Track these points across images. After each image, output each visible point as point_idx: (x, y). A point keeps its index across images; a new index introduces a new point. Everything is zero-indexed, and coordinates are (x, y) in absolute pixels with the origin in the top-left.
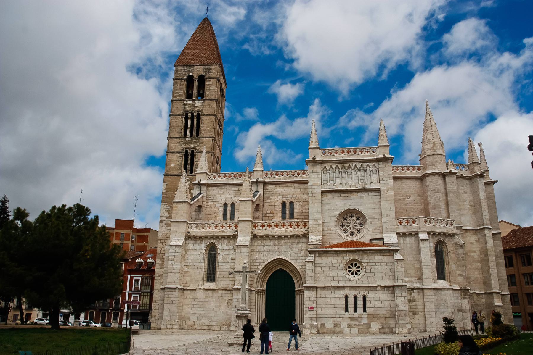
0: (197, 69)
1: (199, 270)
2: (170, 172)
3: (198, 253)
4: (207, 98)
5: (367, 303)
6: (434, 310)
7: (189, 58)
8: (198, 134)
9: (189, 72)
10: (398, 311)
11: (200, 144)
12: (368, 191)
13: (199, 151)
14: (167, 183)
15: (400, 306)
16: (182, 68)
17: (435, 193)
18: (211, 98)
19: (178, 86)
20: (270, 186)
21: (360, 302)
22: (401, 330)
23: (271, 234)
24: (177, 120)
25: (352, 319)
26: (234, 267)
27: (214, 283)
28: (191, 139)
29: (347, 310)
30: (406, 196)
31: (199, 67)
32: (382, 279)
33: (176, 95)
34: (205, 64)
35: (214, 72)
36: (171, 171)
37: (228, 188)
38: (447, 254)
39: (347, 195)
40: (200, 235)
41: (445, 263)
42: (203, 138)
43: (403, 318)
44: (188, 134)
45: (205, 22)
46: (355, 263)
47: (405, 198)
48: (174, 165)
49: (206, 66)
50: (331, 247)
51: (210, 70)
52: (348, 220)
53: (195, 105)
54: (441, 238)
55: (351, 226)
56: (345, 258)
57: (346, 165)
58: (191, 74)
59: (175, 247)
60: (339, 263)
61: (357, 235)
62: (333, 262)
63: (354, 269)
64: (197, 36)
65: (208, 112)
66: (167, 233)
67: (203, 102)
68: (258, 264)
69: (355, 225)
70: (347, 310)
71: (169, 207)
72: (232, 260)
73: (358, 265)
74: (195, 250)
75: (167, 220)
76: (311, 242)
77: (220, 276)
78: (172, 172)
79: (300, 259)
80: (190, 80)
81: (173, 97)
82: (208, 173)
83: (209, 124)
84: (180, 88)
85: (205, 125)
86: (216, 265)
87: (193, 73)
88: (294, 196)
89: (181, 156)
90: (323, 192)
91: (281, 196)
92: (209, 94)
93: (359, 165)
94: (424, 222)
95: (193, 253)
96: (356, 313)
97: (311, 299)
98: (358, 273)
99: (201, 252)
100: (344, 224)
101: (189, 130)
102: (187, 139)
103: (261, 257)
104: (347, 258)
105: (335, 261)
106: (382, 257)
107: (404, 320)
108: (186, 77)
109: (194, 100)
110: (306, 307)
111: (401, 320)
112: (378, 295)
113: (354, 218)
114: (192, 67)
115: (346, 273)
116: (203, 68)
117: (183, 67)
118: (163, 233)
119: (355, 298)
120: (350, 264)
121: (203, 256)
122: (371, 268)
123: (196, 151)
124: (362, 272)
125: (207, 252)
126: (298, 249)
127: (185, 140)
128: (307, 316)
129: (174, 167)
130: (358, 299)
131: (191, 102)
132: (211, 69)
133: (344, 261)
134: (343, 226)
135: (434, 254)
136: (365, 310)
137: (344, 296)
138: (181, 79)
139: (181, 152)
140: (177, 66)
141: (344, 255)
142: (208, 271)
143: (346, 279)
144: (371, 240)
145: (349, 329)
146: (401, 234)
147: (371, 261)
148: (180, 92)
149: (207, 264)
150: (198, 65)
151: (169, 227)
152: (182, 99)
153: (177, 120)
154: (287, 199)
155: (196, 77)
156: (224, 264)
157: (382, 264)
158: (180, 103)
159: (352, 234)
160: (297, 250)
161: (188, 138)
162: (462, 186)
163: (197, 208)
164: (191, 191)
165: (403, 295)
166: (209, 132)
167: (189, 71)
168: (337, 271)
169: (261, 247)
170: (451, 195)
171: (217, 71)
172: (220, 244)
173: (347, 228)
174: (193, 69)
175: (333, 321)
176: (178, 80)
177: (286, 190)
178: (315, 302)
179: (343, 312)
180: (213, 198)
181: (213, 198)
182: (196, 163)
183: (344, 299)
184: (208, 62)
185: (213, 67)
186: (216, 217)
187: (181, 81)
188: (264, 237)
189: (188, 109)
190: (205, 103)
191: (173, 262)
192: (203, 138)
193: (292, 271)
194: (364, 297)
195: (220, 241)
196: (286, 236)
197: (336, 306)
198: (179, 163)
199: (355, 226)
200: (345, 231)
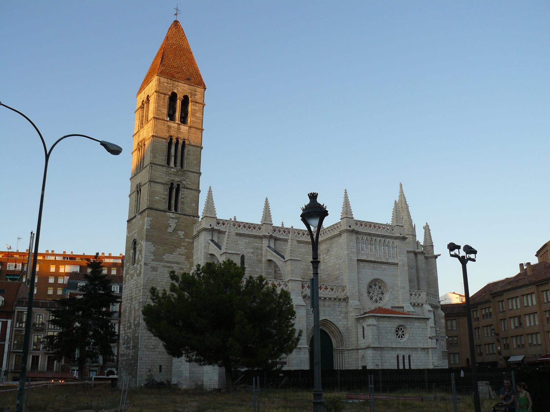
0: (182, 88)
2: (154, 206)
5: (411, 361)
7: (172, 69)
8: (182, 166)
11: (186, 178)
13: (186, 187)
14: (151, 219)
16: (166, 81)
18: (197, 126)
31: (183, 84)
34: (191, 84)
35: (200, 96)
36: (156, 205)
44: (172, 164)
46: (401, 327)
48: (158, 198)
49: (192, 87)
51: (196, 93)
52: (376, 287)
53: (180, 131)
56: (396, 323)
57: (374, 238)
58: (176, 91)
60: (392, 327)
63: (400, 333)
64: (173, 42)
66: (153, 279)
67: (189, 129)
71: (154, 248)
73: (403, 330)
75: (153, 262)
78: (156, 206)
79: (341, 321)
80: (173, 97)
85: (192, 158)
87: (177, 92)
89: (166, 189)
90: (358, 260)
93: (382, 239)
97: (377, 358)
98: (403, 337)
101: (173, 159)
102: (172, 169)
103: (309, 317)
104: (397, 323)
105: (389, 326)
113: (377, 287)
114: (177, 82)
118: (148, 278)
119: (403, 356)
120: (398, 329)
122: (413, 333)
123: (183, 186)
124: (407, 336)
126: (339, 312)
133: (394, 327)
134: (369, 293)
137: (397, 355)
138: (165, 94)
139: (167, 184)
141: (395, 320)
144: (392, 307)
146: (413, 304)
147: (413, 327)
148: (163, 110)
150: (182, 82)
151: (155, 271)
155: (180, 96)
159: (376, 301)
160: (338, 312)
164: (178, 233)
166: (195, 166)
170: (421, 272)
174: (177, 86)
178: (380, 361)
182: (182, 200)
184: (194, 83)
187: (164, 97)
189: (173, 133)
190: (191, 131)
193: (332, 332)
196: (330, 299)
197: (392, 364)
198: (165, 197)
200: (371, 298)
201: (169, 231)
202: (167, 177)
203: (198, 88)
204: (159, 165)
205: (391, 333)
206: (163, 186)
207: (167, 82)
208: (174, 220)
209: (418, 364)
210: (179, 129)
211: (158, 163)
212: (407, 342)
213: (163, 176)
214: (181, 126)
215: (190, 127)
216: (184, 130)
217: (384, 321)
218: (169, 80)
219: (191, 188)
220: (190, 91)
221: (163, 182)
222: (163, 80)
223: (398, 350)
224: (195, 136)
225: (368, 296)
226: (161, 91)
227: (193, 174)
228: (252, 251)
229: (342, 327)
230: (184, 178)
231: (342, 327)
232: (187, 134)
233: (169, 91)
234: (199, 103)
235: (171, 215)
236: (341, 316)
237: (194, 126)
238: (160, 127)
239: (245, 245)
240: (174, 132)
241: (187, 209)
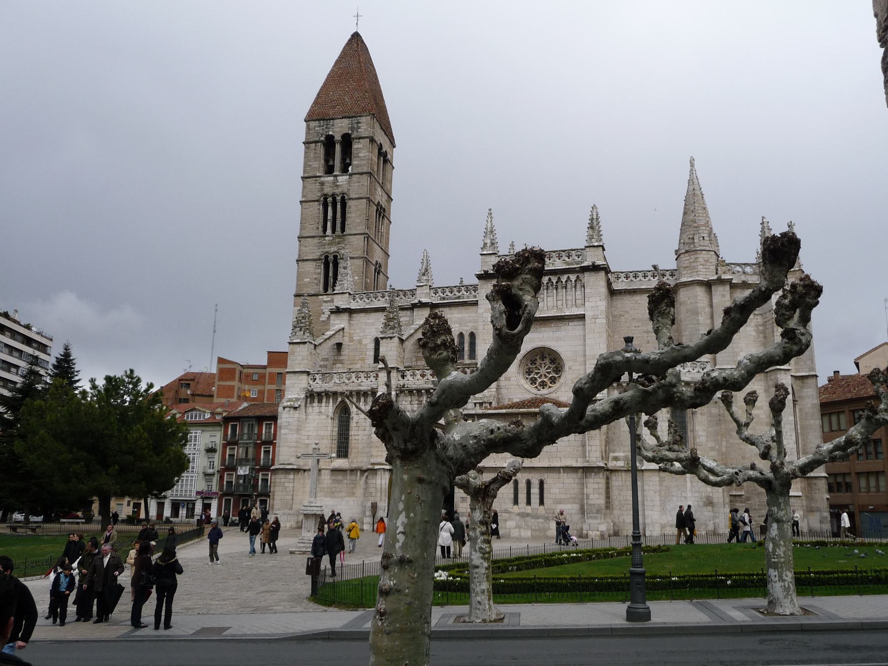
0: (340, 125)
1: (325, 441)
2: (302, 290)
3: (324, 417)
6: (658, 503)
8: (343, 229)
12: (567, 319)
15: (591, 497)
21: (535, 491)
24: (311, 209)
25: (523, 515)
27: (346, 460)
28: (333, 239)
29: (516, 502)
33: (308, 168)
35: (365, 127)
36: (305, 289)
38: (691, 415)
41: (689, 428)
42: (350, 235)
44: (329, 231)
48: (308, 280)
50: (511, 407)
51: (360, 125)
53: (338, 184)
58: (331, 133)
61: (550, 387)
65: (357, 194)
69: (548, 371)
70: (516, 502)
80: (329, 143)
81: (304, 172)
82: (352, 293)
83: (359, 212)
85: (354, 215)
86: (349, 433)
87: (333, 132)
89: (319, 266)
91: (458, 325)
96: (529, 508)
99: (328, 416)
101: (329, 224)
102: (327, 238)
107: (596, 518)
108: (323, 139)
109: (336, 176)
114: (331, 121)
117: (317, 122)
119: (529, 483)
121: (330, 421)
127: (325, 240)
129: (309, 282)
131: (332, 178)
132: (360, 123)
134: (529, 372)
136: (542, 502)
138: (316, 142)
140: (309, 121)
145: (517, 530)
149: (337, 433)
152: (318, 174)
153: (311, 209)
154: (466, 328)
155: (338, 137)
156: (360, 433)
159: (543, 385)
161: (328, 236)
163: (335, 347)
167: (326, 128)
171: (369, 126)
173: (535, 376)
174: (333, 125)
177: (464, 315)
185: (363, 120)
186: (363, 360)
187: (316, 146)
188: (414, 392)
189: (328, 190)
191: (287, 431)
192: (350, 235)
194: (542, 483)
198: (316, 276)
199: (548, 373)
200: (533, 381)
201: (321, 319)
202: (320, 250)
203: (362, 118)
206: (314, 263)
208: (329, 304)
210: (335, 184)
211: (308, 235)
213: (314, 250)
214: (338, 177)
215: (351, 175)
218: (322, 122)
219: (355, 256)
221: (316, 258)
224: (357, 184)
225: (527, 378)
226: (311, 140)
227: (356, 236)
230: (343, 245)
232: (347, 186)
233: (322, 136)
235: (325, 298)
237: (355, 171)
238: (310, 188)
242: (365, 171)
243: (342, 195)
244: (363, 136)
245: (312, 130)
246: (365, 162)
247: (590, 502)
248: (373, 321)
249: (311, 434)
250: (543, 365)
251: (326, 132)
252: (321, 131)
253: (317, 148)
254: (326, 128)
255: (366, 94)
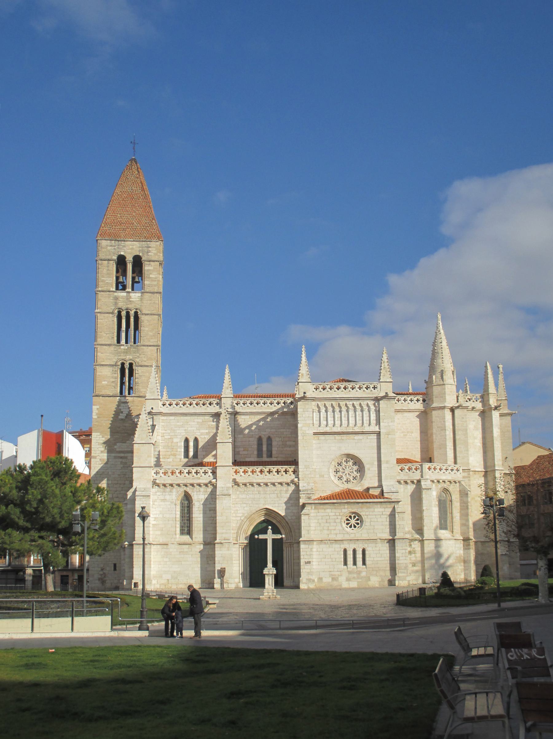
0: (131, 247)
4: (147, 291)
5: (367, 556)
7: (117, 227)
9: (119, 250)
10: (398, 564)
13: (140, 364)
15: (401, 558)
17: (442, 430)
19: (105, 270)
20: (243, 417)
22: (401, 582)
23: (255, 481)
26: (212, 518)
29: (345, 563)
30: (408, 432)
31: (133, 242)
32: (383, 533)
33: (102, 283)
34: (141, 240)
35: (155, 252)
37: (188, 418)
39: (343, 438)
40: (170, 482)
43: (403, 571)
44: (123, 341)
45: (133, 167)
47: (406, 435)
48: (106, 382)
49: (144, 243)
51: (150, 249)
53: (131, 300)
54: (445, 486)
55: (346, 472)
56: (343, 510)
58: (122, 253)
59: (142, 497)
62: (331, 514)
63: (353, 522)
65: (149, 310)
68: (241, 515)
70: (345, 563)
72: (210, 510)
74: (164, 500)
76: (303, 491)
77: (196, 529)
79: (289, 509)
80: (121, 261)
84: (108, 274)
85: (147, 329)
87: (125, 252)
88: (273, 430)
89: (115, 371)
92: (149, 285)
94: (428, 468)
95: (163, 503)
99: (172, 502)
100: (338, 470)
101: (123, 335)
102: (122, 347)
106: (383, 510)
107: (404, 573)
108: (115, 258)
110: (302, 561)
111: (401, 573)
112: (378, 549)
114: (123, 242)
115: (344, 525)
116: (138, 245)
117: (109, 241)
119: (354, 551)
122: (371, 521)
125: (179, 502)
128: (304, 571)
129: (107, 385)
130: (357, 552)
131: (125, 294)
132: (149, 247)
133: (341, 514)
134: (337, 472)
135: (437, 503)
136: (364, 563)
137: (342, 550)
138: (109, 260)
139: (116, 365)
141: (342, 507)
142: (181, 523)
143: (344, 532)
145: (347, 582)
147: (371, 513)
148: (108, 279)
150: (131, 240)
152: (111, 289)
153: (106, 320)
155: (129, 259)
157: (382, 516)
158: (109, 295)
159: (347, 481)
161: (123, 345)
162: (474, 421)
165: (404, 548)
166: (152, 339)
167: (118, 248)
168: (335, 524)
169: (244, 496)
172: (195, 493)
174: (124, 246)
175: (331, 575)
176: (104, 262)
179: (342, 566)
180: (169, 431)
181: (169, 431)
183: (342, 553)
184: (145, 237)
185: (153, 244)
187: (108, 263)
189: (121, 304)
194: (364, 551)
195: (195, 489)
197: (334, 560)
198: (113, 380)
200: (340, 478)
202: (116, 357)
204: (106, 345)
205: (335, 522)
206: (111, 369)
207: (110, 244)
209: (375, 559)
210: (128, 298)
211: (103, 343)
212: (361, 532)
216: (136, 298)
217: (325, 509)
218: (113, 242)
220: (141, 249)
222: (105, 244)
223: (345, 542)
224: (149, 302)
227: (150, 347)
228: (207, 431)
229: (291, 516)
230: (138, 355)
231: (291, 516)
232: (139, 302)
234: (154, 261)
236: (289, 503)
239: (198, 426)
240: (122, 303)
241: (142, 390)
242: (156, 291)
243: (135, 310)
244: (153, 259)
245: (104, 248)
246: (155, 283)
247: (400, 562)
248: (182, 423)
249: (157, 516)
250: (347, 467)
251: (118, 252)
252: (113, 251)
253: (109, 265)
254: (118, 248)
255: (154, 221)
